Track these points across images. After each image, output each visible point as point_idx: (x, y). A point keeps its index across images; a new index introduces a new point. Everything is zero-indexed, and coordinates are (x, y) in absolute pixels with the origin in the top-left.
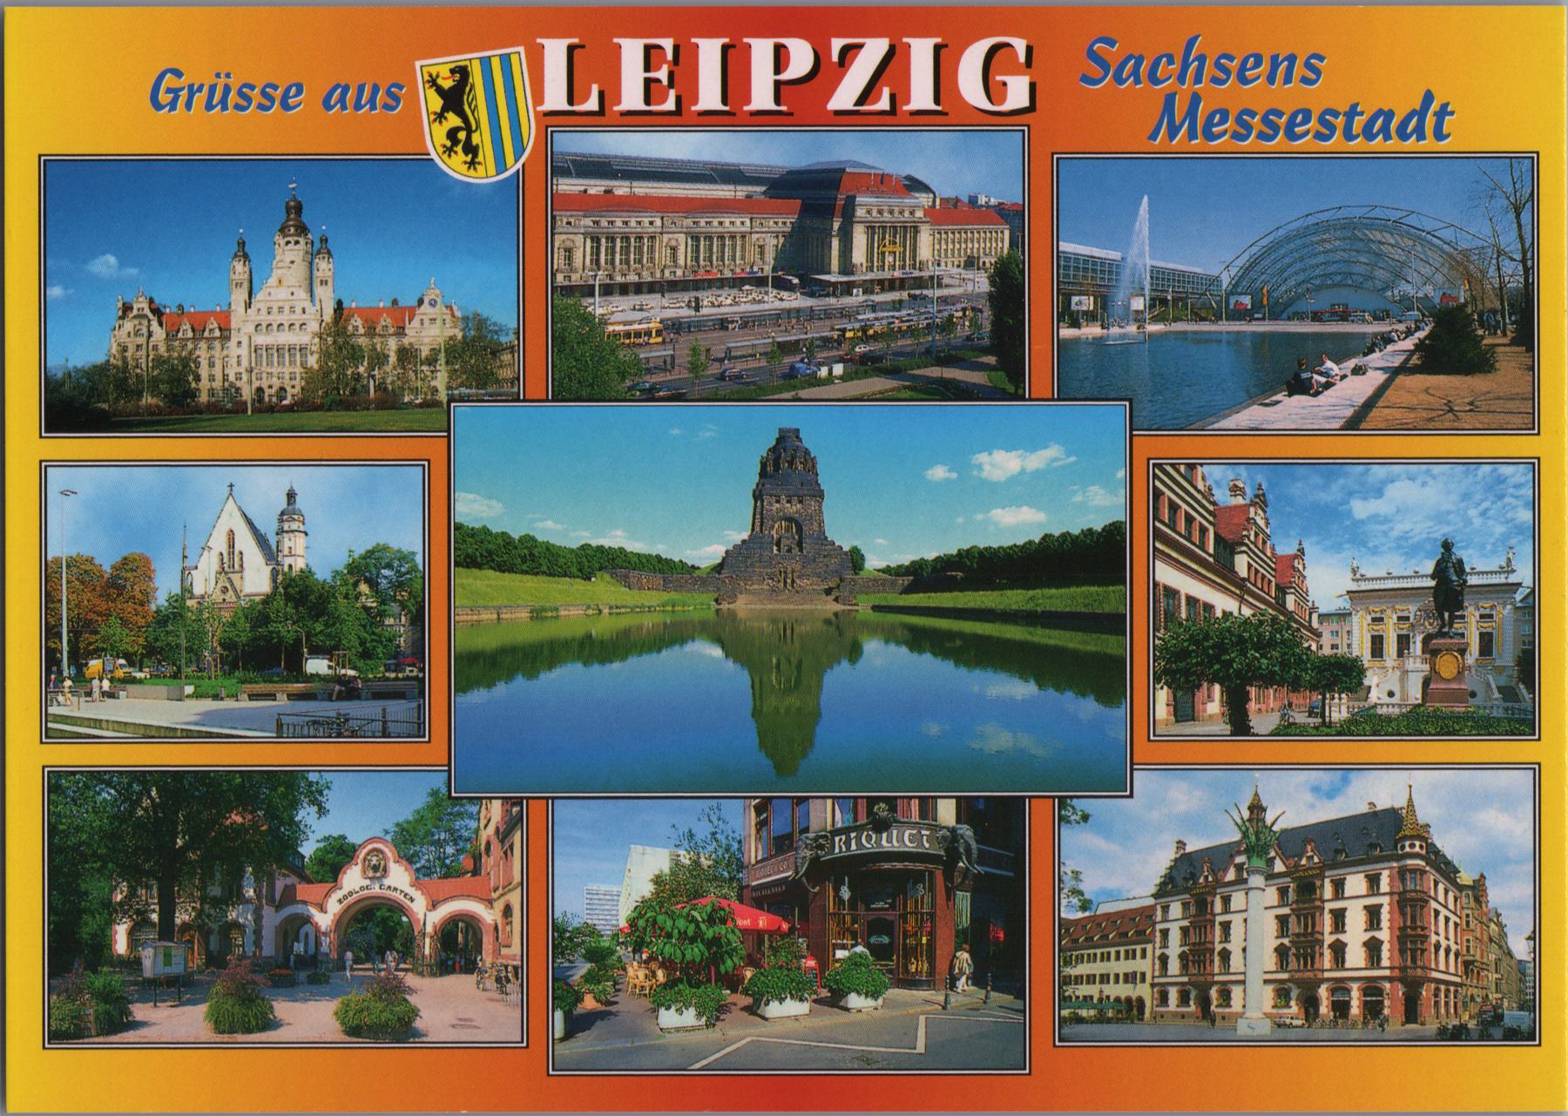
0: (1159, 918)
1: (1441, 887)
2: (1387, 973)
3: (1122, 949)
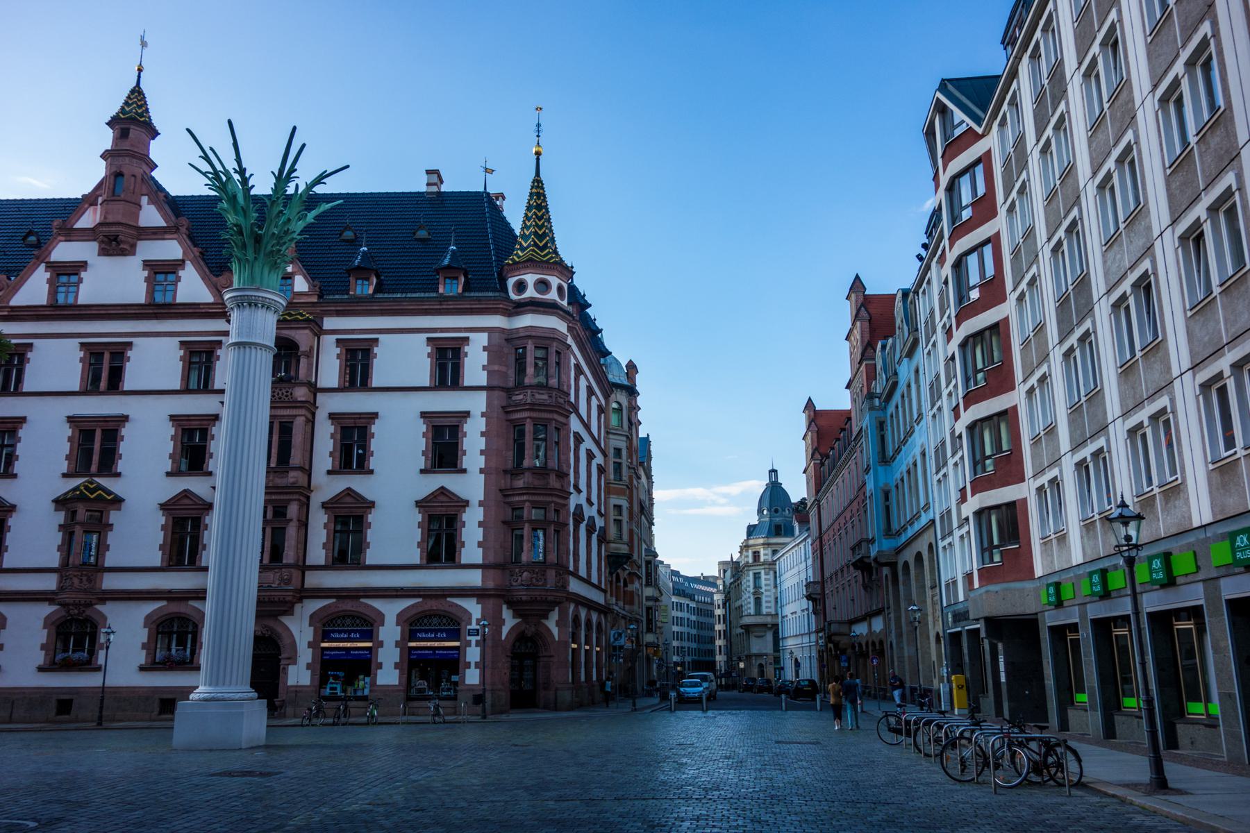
2: (474, 578)
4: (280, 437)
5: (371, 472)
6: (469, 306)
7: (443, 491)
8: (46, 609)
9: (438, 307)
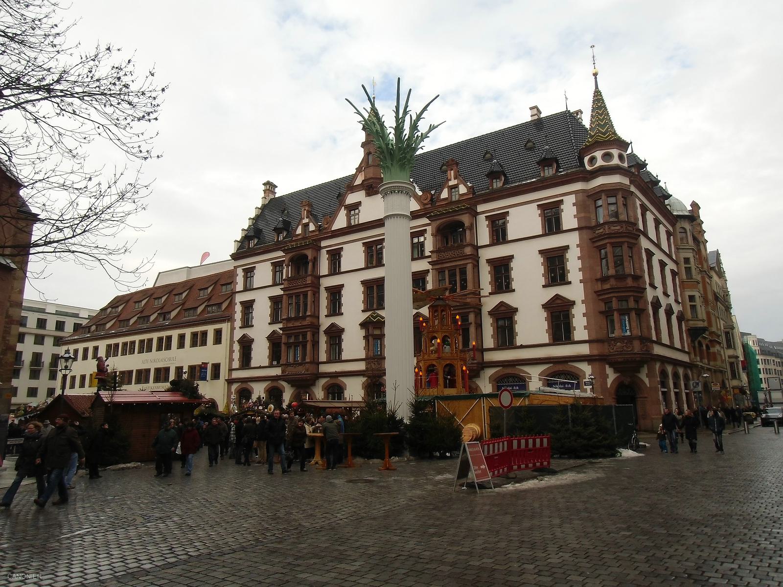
0: (240, 287)
1: (650, 217)
2: (585, 349)
3: (188, 332)
4: (460, 277)
5: (514, 290)
6: (560, 180)
7: (557, 297)
8: (363, 379)
9: (541, 185)
